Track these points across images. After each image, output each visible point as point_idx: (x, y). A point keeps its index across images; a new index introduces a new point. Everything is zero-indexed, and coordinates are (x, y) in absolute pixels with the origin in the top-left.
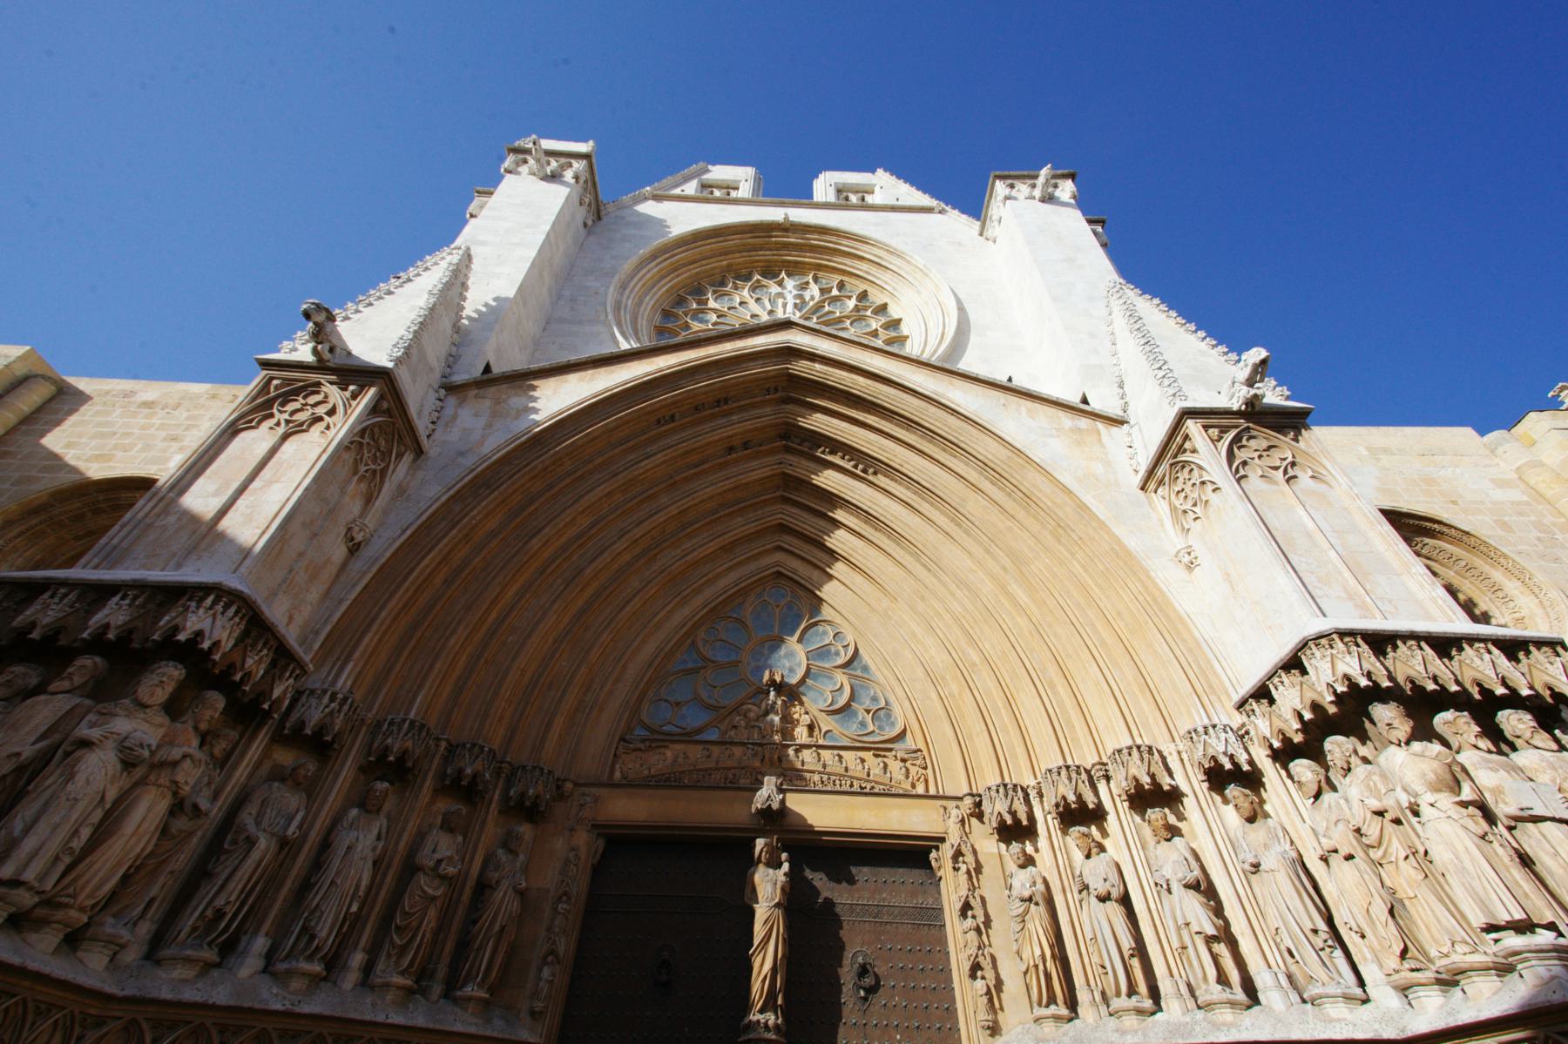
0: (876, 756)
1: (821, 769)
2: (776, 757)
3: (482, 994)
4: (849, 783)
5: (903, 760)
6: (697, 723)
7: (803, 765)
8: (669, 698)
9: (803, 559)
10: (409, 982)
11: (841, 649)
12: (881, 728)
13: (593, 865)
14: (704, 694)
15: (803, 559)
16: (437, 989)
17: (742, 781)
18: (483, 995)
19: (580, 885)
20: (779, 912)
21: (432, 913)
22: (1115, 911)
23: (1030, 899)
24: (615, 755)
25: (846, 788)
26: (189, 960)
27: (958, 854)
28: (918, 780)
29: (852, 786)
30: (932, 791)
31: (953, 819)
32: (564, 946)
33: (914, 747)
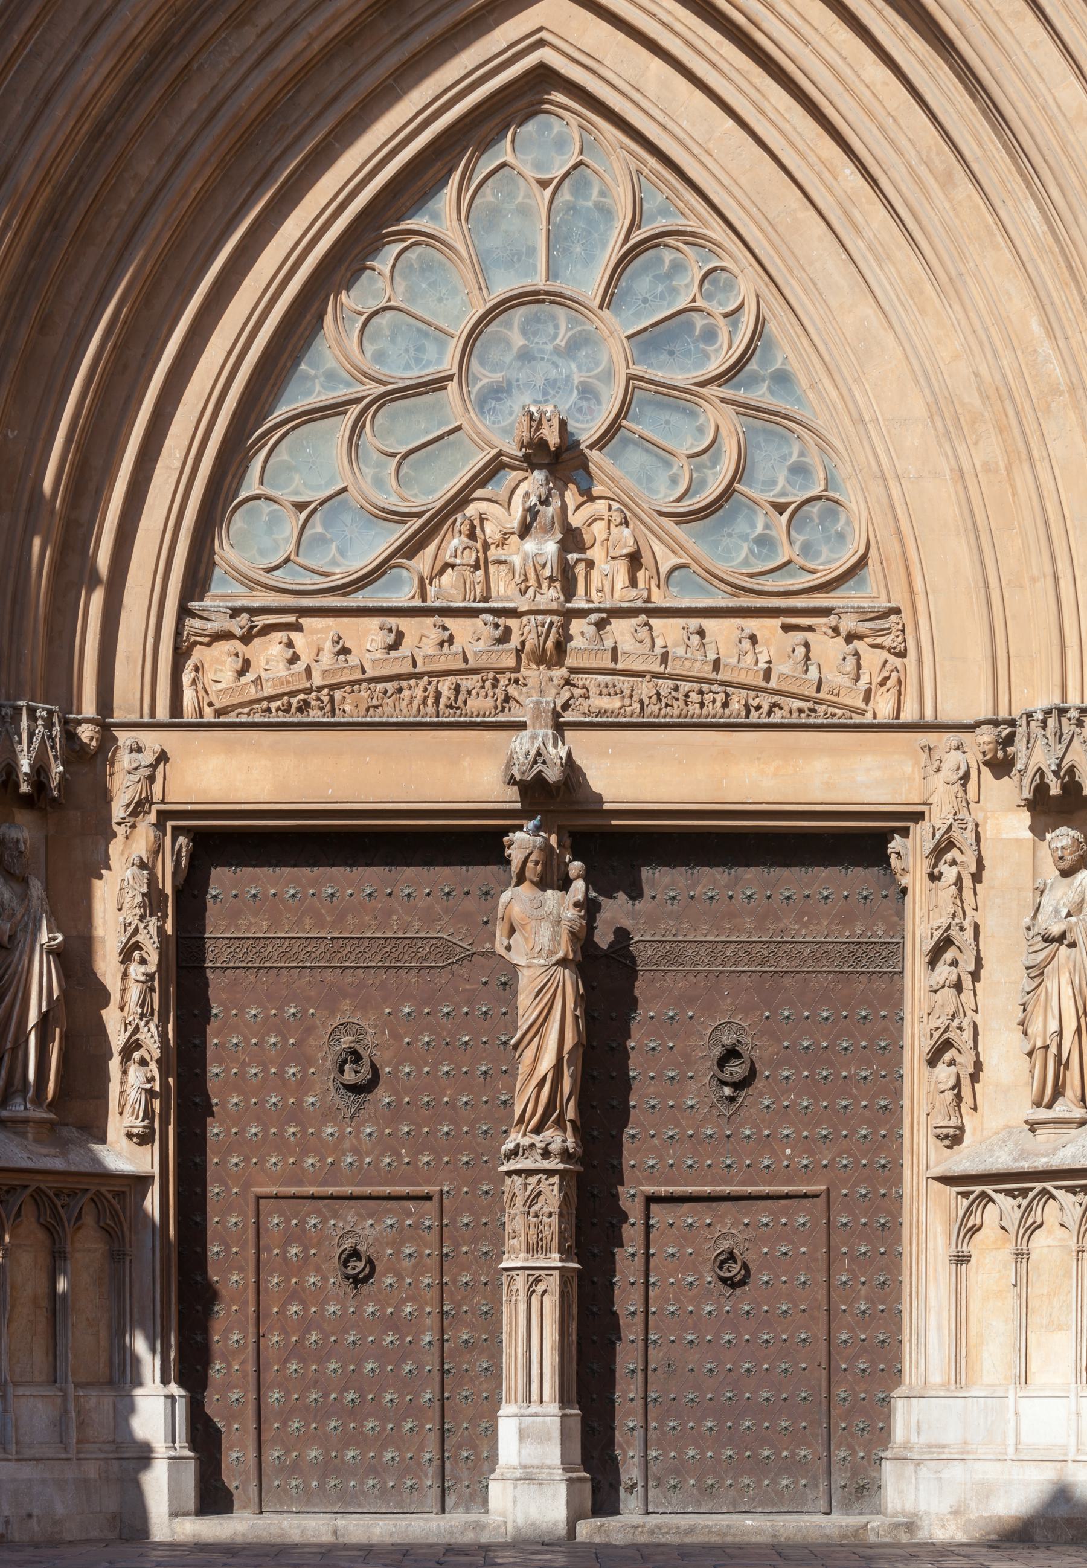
1: (658, 668)
3: (42, 1114)
4: (720, 698)
5: (850, 638)
7: (615, 658)
11: (722, 322)
12: (807, 549)
17: (474, 704)
18: (45, 1115)
20: (567, 975)
23: (1061, 938)
24: (176, 649)
27: (943, 848)
28: (882, 684)
29: (726, 705)
30: (909, 715)
31: (948, 773)
33: (883, 604)
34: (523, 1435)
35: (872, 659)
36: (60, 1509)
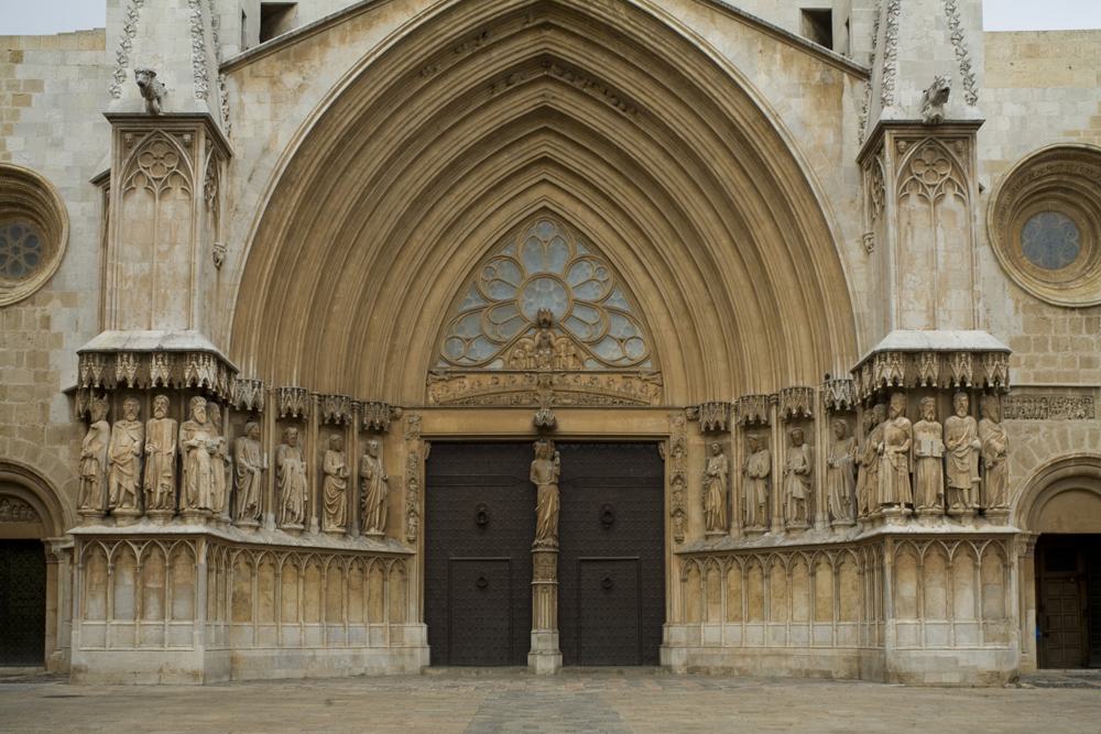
0: (624, 377)
2: (548, 382)
3: (380, 533)
5: (646, 380)
6: (485, 356)
8: (461, 336)
9: (568, 194)
10: (344, 530)
13: (426, 461)
14: (488, 330)
15: (568, 194)
16: (357, 532)
17: (524, 401)
19: (420, 474)
21: (344, 497)
22: (761, 485)
25: (601, 401)
26: (250, 526)
30: (667, 403)
32: (420, 507)
34: (539, 639)
35: (652, 388)
36: (384, 664)
